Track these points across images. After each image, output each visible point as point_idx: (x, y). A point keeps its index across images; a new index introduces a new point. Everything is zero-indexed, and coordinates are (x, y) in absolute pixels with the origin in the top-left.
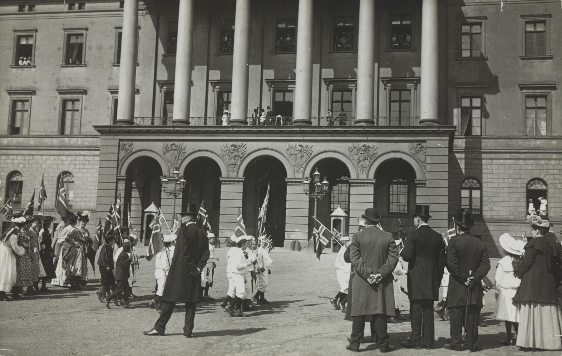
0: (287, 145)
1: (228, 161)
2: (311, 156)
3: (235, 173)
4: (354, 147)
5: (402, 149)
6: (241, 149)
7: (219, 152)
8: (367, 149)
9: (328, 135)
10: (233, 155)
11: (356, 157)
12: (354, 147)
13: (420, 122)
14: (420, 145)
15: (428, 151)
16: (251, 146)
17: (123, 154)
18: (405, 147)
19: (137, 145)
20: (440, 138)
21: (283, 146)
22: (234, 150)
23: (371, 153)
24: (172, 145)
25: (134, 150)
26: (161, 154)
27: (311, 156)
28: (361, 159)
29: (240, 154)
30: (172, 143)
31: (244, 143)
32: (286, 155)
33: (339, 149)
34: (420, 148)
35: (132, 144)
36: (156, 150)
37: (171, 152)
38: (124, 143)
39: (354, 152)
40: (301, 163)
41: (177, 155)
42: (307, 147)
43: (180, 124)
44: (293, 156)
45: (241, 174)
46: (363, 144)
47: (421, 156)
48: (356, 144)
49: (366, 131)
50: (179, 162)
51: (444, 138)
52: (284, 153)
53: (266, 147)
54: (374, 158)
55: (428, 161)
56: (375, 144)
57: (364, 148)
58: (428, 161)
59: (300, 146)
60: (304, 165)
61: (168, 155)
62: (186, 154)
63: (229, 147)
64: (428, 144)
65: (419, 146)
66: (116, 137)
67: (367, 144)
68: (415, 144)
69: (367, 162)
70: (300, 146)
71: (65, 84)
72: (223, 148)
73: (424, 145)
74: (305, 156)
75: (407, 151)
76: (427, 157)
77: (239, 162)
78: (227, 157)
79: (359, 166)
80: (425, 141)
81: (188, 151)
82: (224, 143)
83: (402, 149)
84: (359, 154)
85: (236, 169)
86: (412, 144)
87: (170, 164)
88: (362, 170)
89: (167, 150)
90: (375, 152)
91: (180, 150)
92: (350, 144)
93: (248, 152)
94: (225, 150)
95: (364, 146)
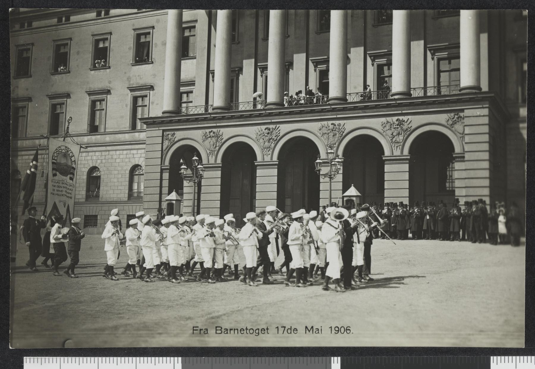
0: (319, 124)
1: (262, 144)
2: (344, 134)
5: (437, 121)
6: (274, 132)
7: (254, 137)
8: (401, 123)
9: (360, 111)
10: (267, 138)
11: (389, 133)
12: (388, 122)
13: (460, 90)
14: (457, 115)
15: (467, 121)
16: (284, 128)
17: (166, 143)
18: (442, 118)
19: (179, 135)
21: (314, 126)
22: (268, 133)
23: (405, 127)
24: (210, 132)
25: (176, 140)
26: (201, 141)
27: (344, 134)
28: (394, 134)
29: (274, 137)
30: (210, 130)
31: (278, 126)
32: (318, 134)
33: (374, 126)
34: (458, 118)
35: (174, 134)
36: (195, 138)
37: (210, 139)
38: (167, 133)
41: (215, 141)
44: (325, 136)
46: (396, 118)
47: (458, 127)
48: (389, 119)
49: (399, 103)
50: (217, 148)
52: (316, 133)
53: (299, 128)
54: (409, 132)
56: (409, 117)
57: (397, 123)
58: (466, 132)
59: (332, 124)
60: (337, 144)
61: (207, 142)
62: (223, 141)
63: (264, 130)
64: (467, 113)
65: (456, 116)
66: (160, 128)
67: (401, 118)
68: (452, 114)
69: (401, 138)
70: (332, 124)
71: (135, 82)
72: (258, 131)
73: (461, 114)
74: (338, 135)
75: (444, 122)
76: (465, 127)
77: (273, 145)
78: (261, 141)
79: (393, 142)
80: (462, 111)
81: (225, 138)
83: (437, 121)
84: (393, 129)
85: (270, 152)
86: (449, 114)
87: (208, 152)
88: (396, 145)
89: (206, 137)
90: (410, 126)
91: (218, 136)
92: (383, 120)
93: (281, 135)
94: (259, 133)
95: (397, 120)
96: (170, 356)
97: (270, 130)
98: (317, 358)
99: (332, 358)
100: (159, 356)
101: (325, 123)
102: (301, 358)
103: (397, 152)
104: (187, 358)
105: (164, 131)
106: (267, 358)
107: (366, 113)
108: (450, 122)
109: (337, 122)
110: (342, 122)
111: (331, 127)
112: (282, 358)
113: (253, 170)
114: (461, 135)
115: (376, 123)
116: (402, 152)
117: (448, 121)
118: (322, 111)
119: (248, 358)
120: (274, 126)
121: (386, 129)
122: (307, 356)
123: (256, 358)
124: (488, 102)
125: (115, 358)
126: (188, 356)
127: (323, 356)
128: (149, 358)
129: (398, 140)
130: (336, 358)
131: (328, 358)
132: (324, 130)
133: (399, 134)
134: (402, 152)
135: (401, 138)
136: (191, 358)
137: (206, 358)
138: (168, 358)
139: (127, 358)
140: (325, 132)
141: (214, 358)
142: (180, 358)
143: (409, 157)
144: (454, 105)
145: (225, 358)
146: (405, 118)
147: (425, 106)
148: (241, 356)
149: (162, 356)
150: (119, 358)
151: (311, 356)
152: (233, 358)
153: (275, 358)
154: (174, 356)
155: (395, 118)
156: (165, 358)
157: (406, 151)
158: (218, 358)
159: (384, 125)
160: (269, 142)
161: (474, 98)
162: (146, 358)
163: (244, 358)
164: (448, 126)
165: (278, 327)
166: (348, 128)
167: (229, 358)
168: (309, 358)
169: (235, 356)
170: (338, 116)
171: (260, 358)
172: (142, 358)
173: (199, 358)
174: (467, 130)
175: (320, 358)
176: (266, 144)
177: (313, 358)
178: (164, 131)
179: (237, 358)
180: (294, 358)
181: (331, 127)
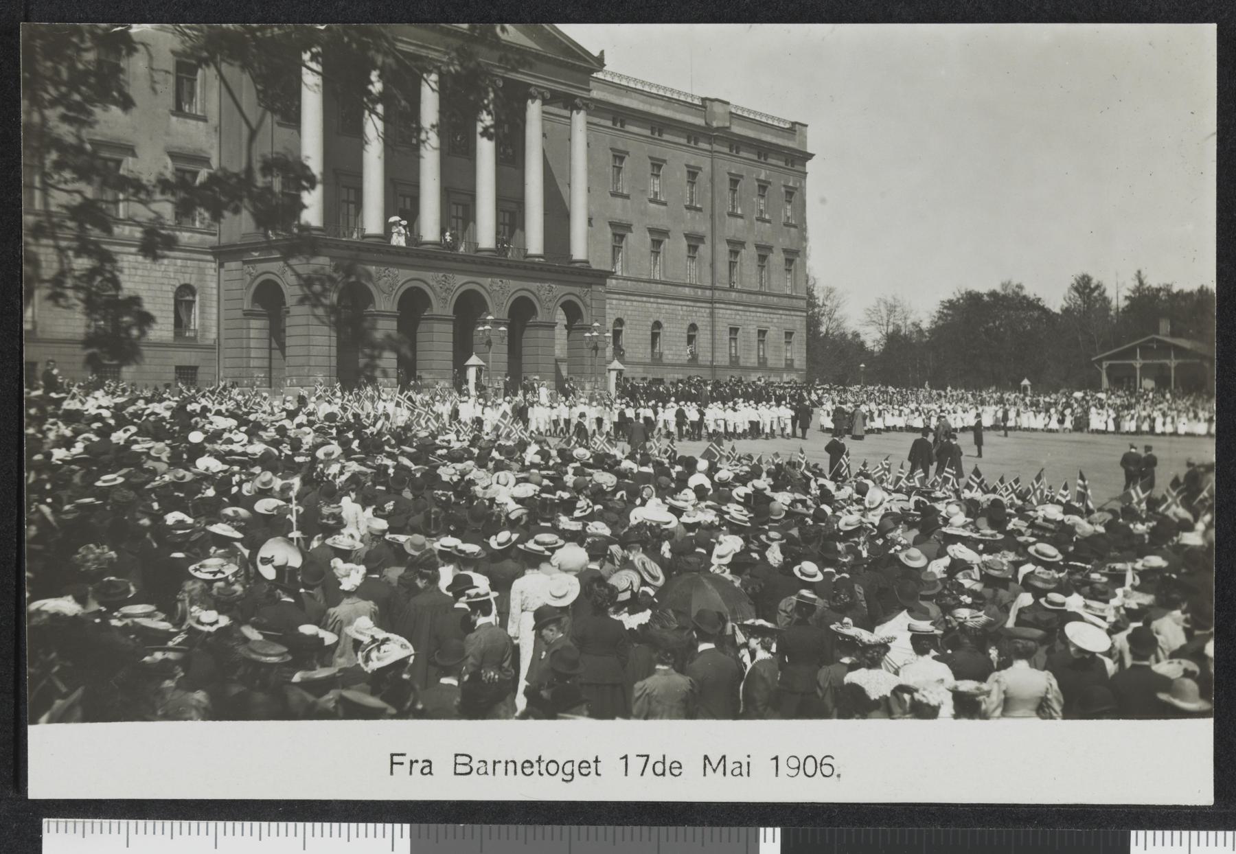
96: (385, 822)
98: (725, 829)
99: (762, 829)
100: (358, 821)
102: (690, 829)
104: (424, 826)
106: (610, 828)
112: (645, 828)
119: (566, 828)
122: (702, 824)
123: (584, 828)
125: (256, 824)
126: (427, 822)
127: (740, 824)
128: (335, 825)
130: (769, 830)
131: (751, 829)
136: (433, 826)
137: (469, 826)
138: (379, 826)
139: (282, 825)
141: (486, 827)
142: (407, 827)
145: (512, 827)
148: (549, 823)
149: (366, 820)
150: (265, 824)
151: (711, 824)
152: (530, 828)
153: (628, 829)
154: (393, 822)
156: (371, 826)
158: (495, 827)
162: (327, 825)
163: (557, 828)
165: (626, 757)
167: (521, 828)
168: (708, 829)
169: (536, 823)
171: (592, 828)
172: (318, 825)
173: (450, 826)
175: (734, 830)
177: (716, 829)
179: (539, 828)
180: (672, 829)
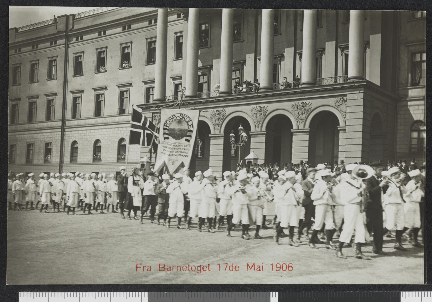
0: (251, 107)
1: (214, 122)
2: (267, 114)
3: (219, 130)
4: (296, 105)
6: (222, 113)
8: (304, 105)
9: (278, 97)
10: (217, 117)
11: (296, 112)
12: (296, 105)
15: (348, 103)
16: (228, 110)
18: (331, 101)
20: (358, 92)
22: (218, 114)
23: (307, 108)
28: (300, 113)
31: (224, 109)
34: (343, 101)
38: (155, 115)
39: (296, 109)
40: (260, 120)
42: (264, 107)
43: (188, 98)
45: (222, 132)
46: (302, 101)
47: (343, 107)
48: (297, 102)
49: (302, 91)
51: (361, 92)
54: (309, 112)
55: (347, 111)
56: (310, 101)
57: (301, 105)
59: (259, 107)
60: (262, 121)
64: (348, 97)
65: (342, 100)
67: (304, 101)
68: (339, 98)
69: (304, 116)
70: (259, 107)
73: (345, 98)
75: (333, 104)
77: (221, 123)
78: (214, 119)
80: (345, 95)
82: (212, 110)
83: (328, 104)
84: (299, 110)
85: (219, 128)
86: (337, 98)
88: (301, 122)
90: (310, 107)
92: (293, 103)
93: (226, 115)
95: (302, 103)
97: (219, 111)
101: (255, 106)
103: (301, 127)
105: (153, 113)
107: (281, 98)
108: (337, 104)
109: (262, 106)
110: (265, 105)
111: (259, 109)
113: (209, 139)
114: (344, 114)
115: (287, 105)
116: (304, 127)
117: (336, 103)
118: (252, 97)
120: (221, 109)
121: (294, 109)
124: (363, 89)
129: (302, 118)
132: (254, 111)
133: (303, 113)
134: (304, 127)
135: (304, 116)
140: (254, 113)
143: (309, 130)
144: (340, 91)
146: (307, 102)
147: (320, 93)
155: (300, 102)
157: (307, 126)
159: (293, 107)
160: (218, 120)
161: (353, 86)
164: (336, 107)
166: (270, 110)
170: (263, 101)
174: (348, 110)
176: (217, 121)
178: (153, 113)
181: (259, 109)
